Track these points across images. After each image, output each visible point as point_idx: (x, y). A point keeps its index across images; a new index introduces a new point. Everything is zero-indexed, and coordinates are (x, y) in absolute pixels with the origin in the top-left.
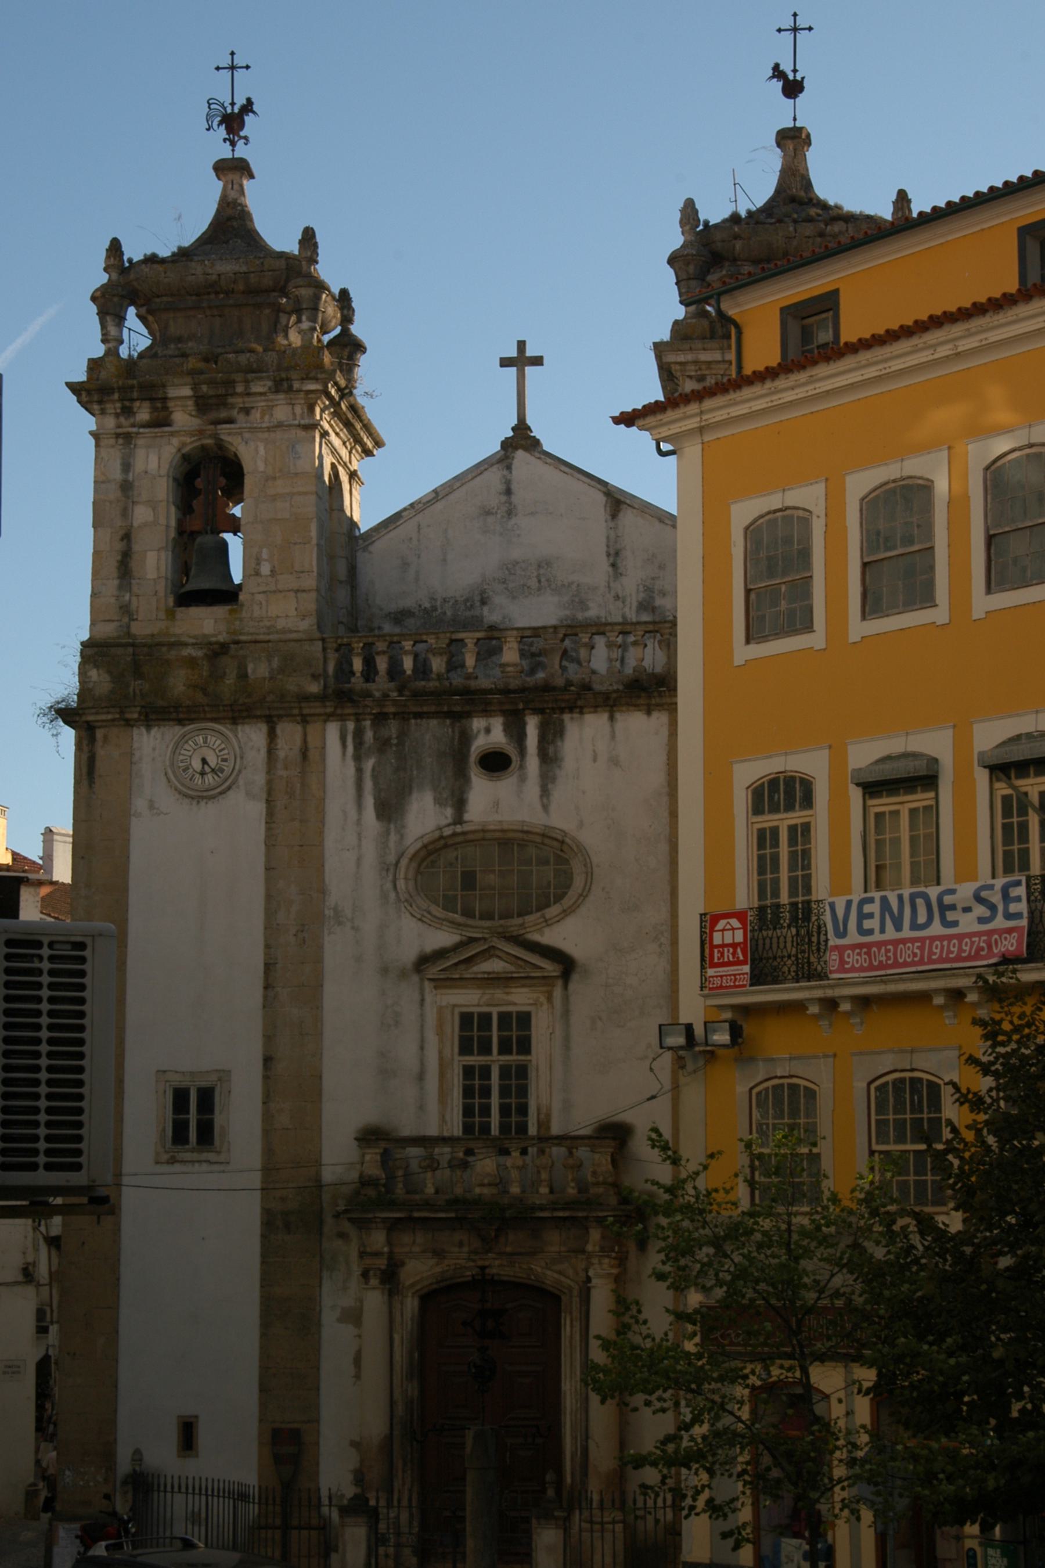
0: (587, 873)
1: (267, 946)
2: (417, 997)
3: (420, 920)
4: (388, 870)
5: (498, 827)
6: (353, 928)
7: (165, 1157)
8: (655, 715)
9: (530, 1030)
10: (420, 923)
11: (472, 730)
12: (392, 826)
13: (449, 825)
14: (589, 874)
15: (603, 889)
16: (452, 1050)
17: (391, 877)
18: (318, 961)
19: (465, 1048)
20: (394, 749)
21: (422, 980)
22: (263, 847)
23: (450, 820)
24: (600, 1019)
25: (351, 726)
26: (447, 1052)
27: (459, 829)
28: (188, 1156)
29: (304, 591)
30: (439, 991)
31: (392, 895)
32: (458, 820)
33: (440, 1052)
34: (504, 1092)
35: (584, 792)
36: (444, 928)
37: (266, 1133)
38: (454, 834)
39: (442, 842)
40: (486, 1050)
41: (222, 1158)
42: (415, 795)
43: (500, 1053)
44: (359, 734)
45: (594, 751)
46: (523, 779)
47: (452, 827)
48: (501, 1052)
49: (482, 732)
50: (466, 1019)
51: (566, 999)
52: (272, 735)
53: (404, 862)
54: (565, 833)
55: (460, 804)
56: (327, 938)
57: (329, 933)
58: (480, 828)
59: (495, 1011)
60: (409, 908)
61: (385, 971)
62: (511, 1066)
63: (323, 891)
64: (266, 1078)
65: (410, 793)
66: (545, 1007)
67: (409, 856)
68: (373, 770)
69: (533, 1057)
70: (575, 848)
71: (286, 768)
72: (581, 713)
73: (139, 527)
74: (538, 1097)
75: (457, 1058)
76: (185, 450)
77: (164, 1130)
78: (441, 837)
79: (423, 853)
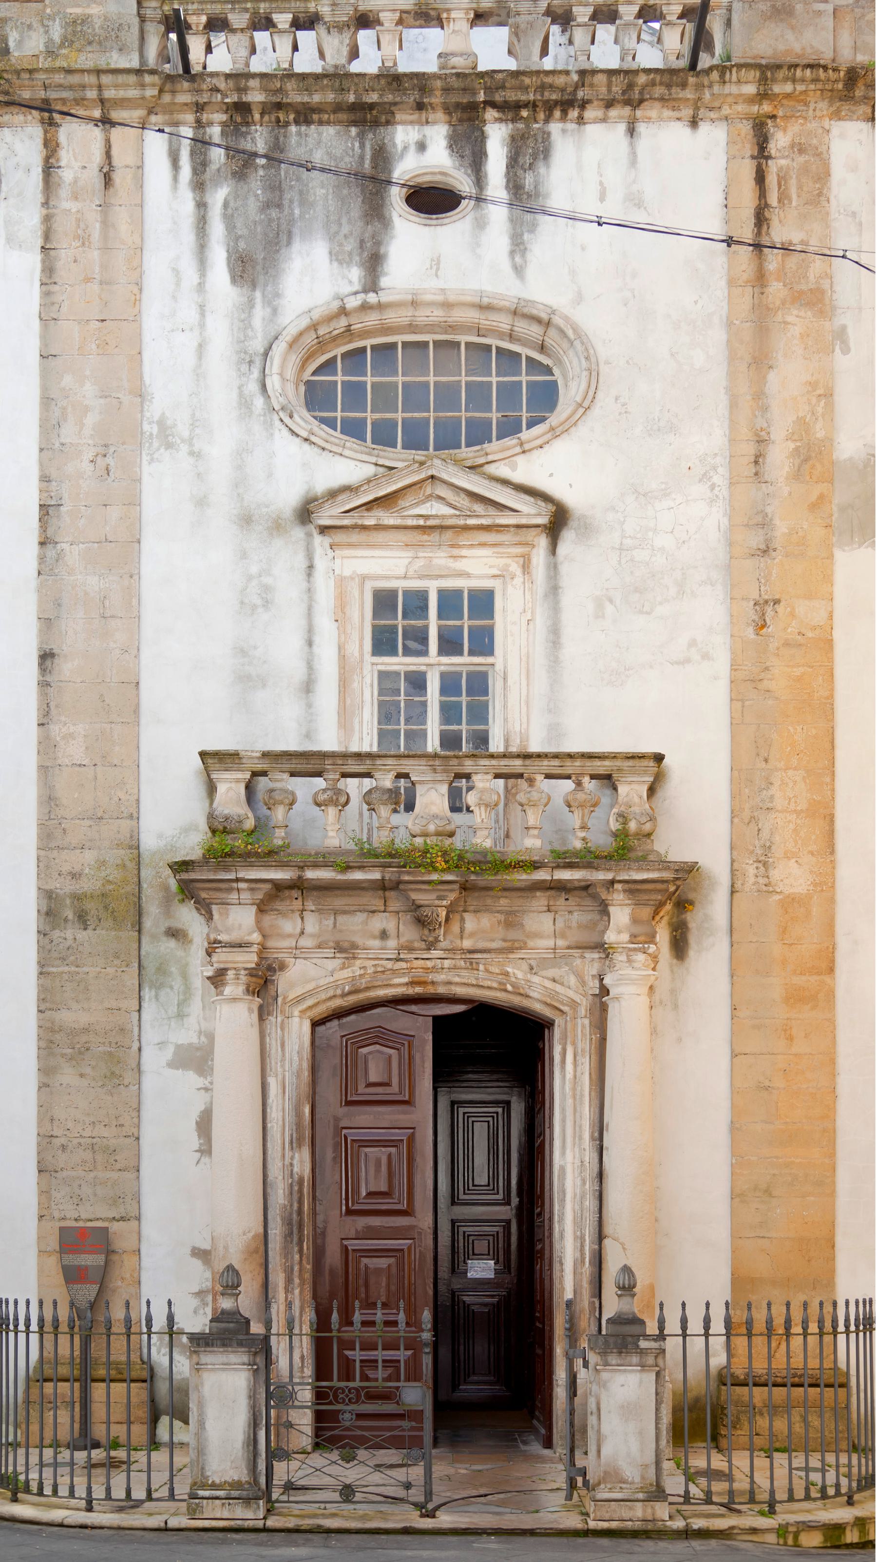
0: (590, 370)
1: (45, 479)
2: (300, 561)
3: (306, 440)
4: (251, 362)
5: (440, 298)
6: (192, 453)
8: (704, 128)
9: (492, 617)
10: (306, 446)
11: (395, 145)
12: (258, 294)
13: (356, 293)
14: (593, 374)
15: (617, 399)
16: (361, 646)
17: (256, 374)
18: (134, 502)
20: (261, 172)
21: (309, 535)
22: (36, 324)
23: (357, 287)
24: (611, 601)
25: (187, 132)
26: (353, 649)
27: (372, 298)
30: (338, 552)
31: (259, 402)
32: (372, 285)
33: (340, 648)
34: (449, 713)
35: (583, 248)
36: (347, 452)
37: (44, 770)
38: (365, 307)
39: (343, 322)
42: (297, 245)
44: (201, 143)
45: (601, 183)
46: (481, 224)
47: (362, 295)
48: (442, 651)
49: (413, 148)
51: (553, 569)
52: (51, 147)
53: (279, 349)
54: (554, 312)
56: (146, 469)
57: (151, 461)
58: (410, 297)
59: (433, 588)
60: (287, 420)
61: (246, 520)
62: (460, 674)
63: (140, 394)
64: (44, 685)
65: (289, 243)
66: (519, 580)
67: (289, 338)
68: (226, 205)
69: (498, 659)
70: (570, 333)
71: (75, 197)
72: (580, 120)
74: (506, 720)
75: (368, 658)
78: (343, 311)
79: (310, 339)
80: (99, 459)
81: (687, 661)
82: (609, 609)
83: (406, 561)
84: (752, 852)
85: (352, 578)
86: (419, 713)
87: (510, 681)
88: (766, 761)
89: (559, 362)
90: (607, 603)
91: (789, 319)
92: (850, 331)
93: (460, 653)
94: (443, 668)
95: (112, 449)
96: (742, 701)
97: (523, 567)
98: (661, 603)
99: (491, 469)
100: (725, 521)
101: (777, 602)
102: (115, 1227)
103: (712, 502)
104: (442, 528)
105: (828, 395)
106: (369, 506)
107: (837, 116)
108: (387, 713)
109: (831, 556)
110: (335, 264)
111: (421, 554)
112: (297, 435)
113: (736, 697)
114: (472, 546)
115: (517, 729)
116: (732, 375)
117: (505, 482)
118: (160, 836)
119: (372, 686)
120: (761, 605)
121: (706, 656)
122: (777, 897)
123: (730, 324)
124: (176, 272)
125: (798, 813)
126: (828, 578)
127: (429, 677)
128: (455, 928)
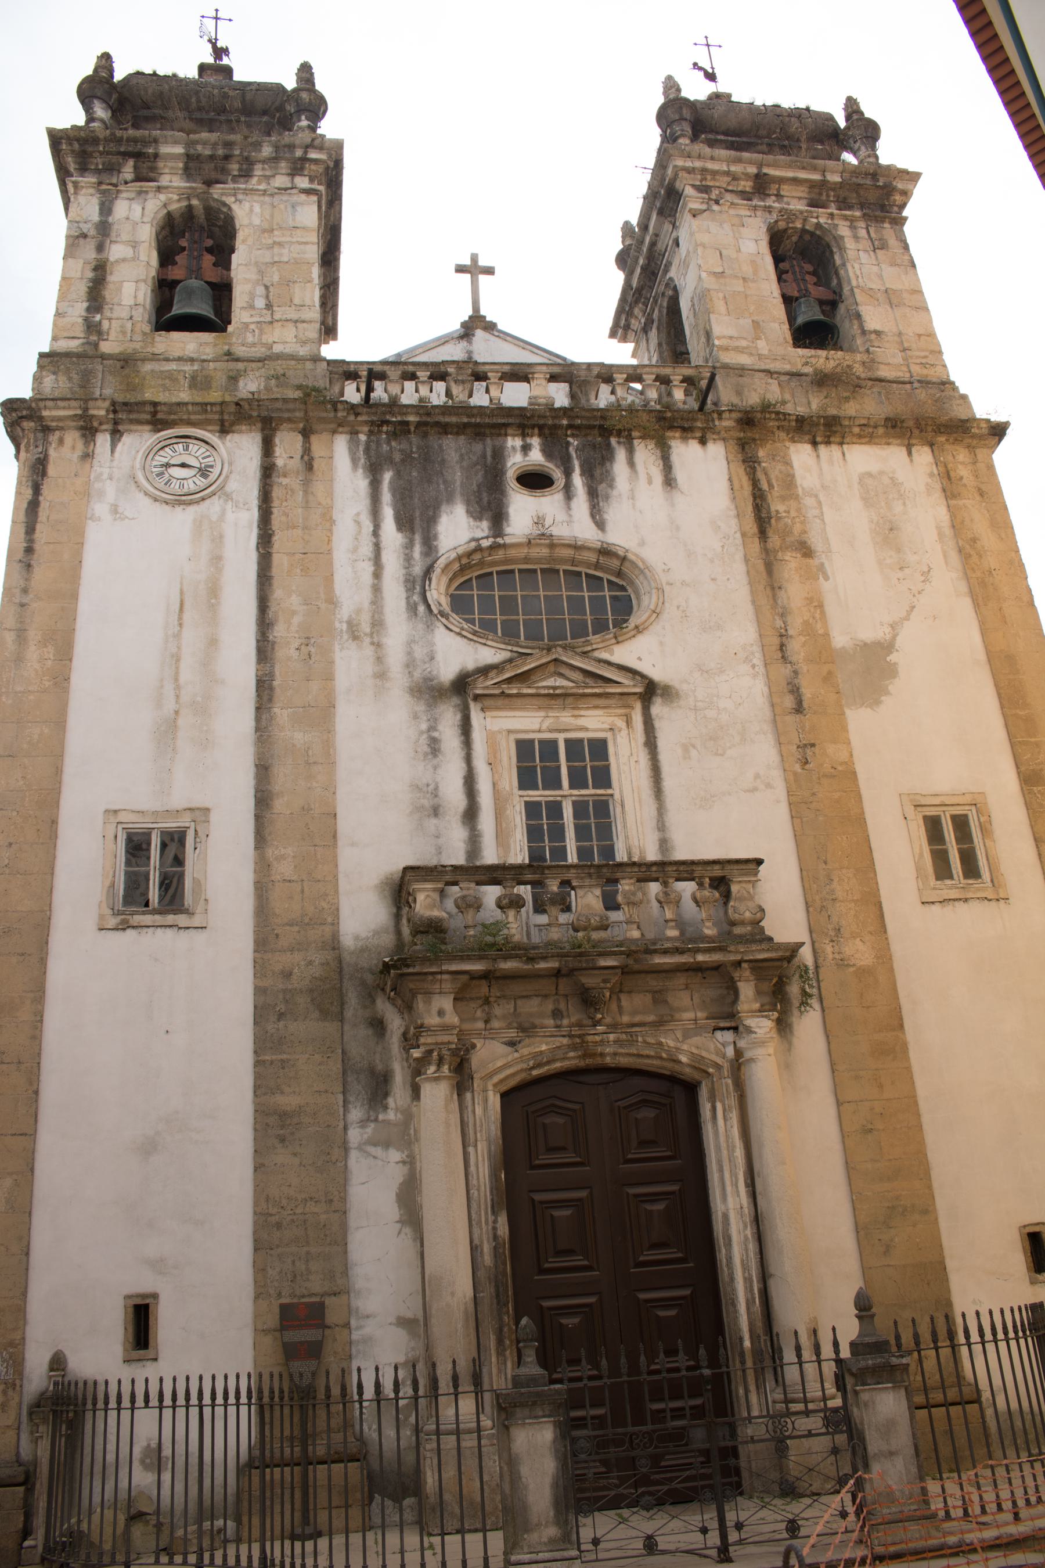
6: (372, 643)
7: (112, 922)
10: (458, 638)
13: (487, 537)
15: (678, 607)
19: (526, 779)
24: (694, 746)
27: (500, 540)
28: (148, 919)
29: (304, 322)
31: (421, 608)
33: (494, 785)
34: (582, 833)
39: (477, 557)
40: (554, 782)
41: (197, 921)
43: (571, 787)
45: (648, 474)
50: (524, 748)
54: (627, 551)
55: (498, 517)
66: (624, 732)
67: (442, 566)
73: (117, 261)
76: (174, 207)
77: (113, 885)
79: (456, 566)
80: (303, 647)
81: (755, 789)
82: (694, 753)
83: (540, 720)
84: (827, 934)
85: (500, 732)
86: (558, 833)
87: (627, 808)
88: (825, 863)
89: (632, 583)
90: (691, 748)
91: (787, 558)
92: (827, 565)
93: (586, 787)
94: (574, 798)
95: (312, 641)
96: (801, 818)
97: (627, 722)
98: (730, 748)
99: (596, 654)
100: (766, 689)
101: (813, 745)
102: (328, 1301)
103: (755, 676)
104: (565, 695)
105: (821, 606)
106: (509, 681)
107: (793, 440)
108: (534, 833)
109: (843, 714)
110: (471, 520)
111: (551, 714)
112: (451, 630)
113: (795, 815)
114: (588, 708)
115: (637, 844)
116: (753, 593)
117: (609, 663)
118: (357, 938)
119: (521, 813)
120: (803, 747)
121: (769, 786)
122: (852, 969)
123: (746, 560)
124: (358, 523)
125: (856, 901)
126: (844, 728)
127: (564, 804)
128: (614, 1006)
